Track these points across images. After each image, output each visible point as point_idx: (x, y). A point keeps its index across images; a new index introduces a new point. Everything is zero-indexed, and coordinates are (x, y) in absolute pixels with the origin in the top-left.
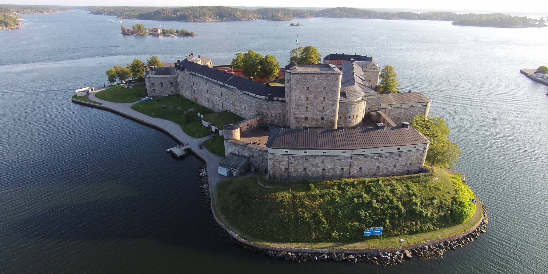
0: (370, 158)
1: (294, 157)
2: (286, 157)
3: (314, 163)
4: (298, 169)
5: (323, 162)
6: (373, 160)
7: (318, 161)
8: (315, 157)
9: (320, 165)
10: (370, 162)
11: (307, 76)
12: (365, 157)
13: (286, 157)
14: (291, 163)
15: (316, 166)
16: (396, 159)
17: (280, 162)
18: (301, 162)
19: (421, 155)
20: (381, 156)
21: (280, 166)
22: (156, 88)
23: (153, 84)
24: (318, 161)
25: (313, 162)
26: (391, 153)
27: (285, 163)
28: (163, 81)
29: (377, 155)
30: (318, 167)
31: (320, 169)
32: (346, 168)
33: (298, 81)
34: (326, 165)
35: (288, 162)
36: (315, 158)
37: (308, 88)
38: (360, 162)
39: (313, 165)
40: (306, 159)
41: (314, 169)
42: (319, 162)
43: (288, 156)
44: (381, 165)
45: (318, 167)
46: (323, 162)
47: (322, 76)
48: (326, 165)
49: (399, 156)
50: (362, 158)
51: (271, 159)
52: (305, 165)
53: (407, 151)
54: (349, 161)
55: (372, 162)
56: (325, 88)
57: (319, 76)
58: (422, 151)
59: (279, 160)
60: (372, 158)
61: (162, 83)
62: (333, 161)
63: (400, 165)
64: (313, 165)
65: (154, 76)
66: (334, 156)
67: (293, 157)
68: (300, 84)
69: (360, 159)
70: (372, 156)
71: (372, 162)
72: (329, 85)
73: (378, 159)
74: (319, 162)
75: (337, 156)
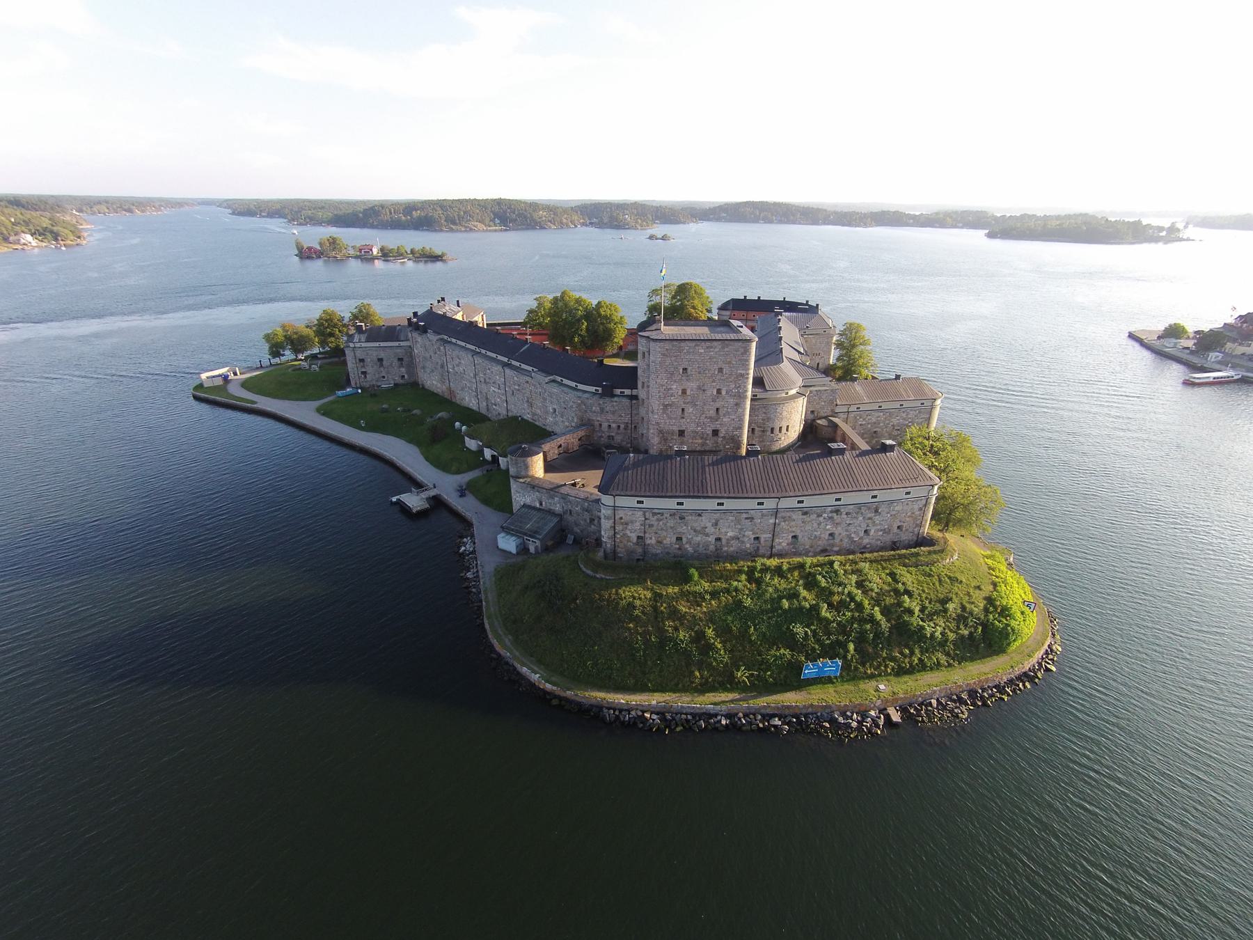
3: (697, 526)
7: (706, 521)
9: (710, 530)
11: (683, 344)
12: (805, 513)
18: (671, 523)
20: (837, 512)
22: (369, 370)
23: (362, 360)
24: (706, 521)
25: (695, 525)
26: (859, 506)
27: (637, 526)
28: (382, 355)
30: (707, 535)
31: (712, 539)
32: (765, 537)
34: (723, 530)
35: (644, 525)
37: (685, 369)
40: (682, 518)
41: (699, 539)
42: (709, 525)
43: (645, 510)
45: (707, 535)
46: (716, 524)
47: (715, 343)
48: (723, 530)
49: (876, 511)
50: (797, 516)
51: (607, 518)
52: (679, 530)
53: (892, 502)
54: (772, 521)
55: (819, 524)
56: (721, 370)
57: (708, 344)
59: (625, 519)
60: (819, 516)
61: (380, 360)
62: (738, 521)
65: (364, 345)
66: (739, 512)
67: (654, 514)
68: (668, 361)
70: (819, 511)
74: (709, 525)
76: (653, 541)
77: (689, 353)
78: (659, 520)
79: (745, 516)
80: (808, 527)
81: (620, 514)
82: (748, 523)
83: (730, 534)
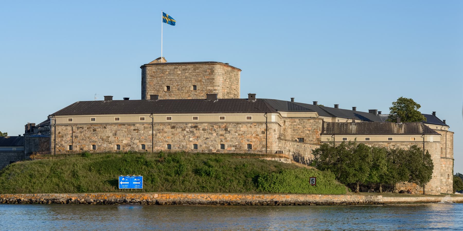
0: (179, 130)
1: (80, 127)
2: (69, 128)
4: (85, 145)
5: (116, 134)
6: (185, 132)
8: (104, 126)
9: (112, 139)
10: (181, 137)
11: (165, 68)
12: (173, 127)
13: (69, 128)
14: (76, 137)
15: (106, 140)
16: (222, 135)
17: (63, 137)
18: (88, 134)
19: (263, 133)
20: (196, 127)
21: (63, 143)
24: (108, 132)
25: (103, 135)
27: (69, 138)
29: (190, 125)
32: (148, 144)
33: (151, 76)
34: (120, 139)
35: (72, 137)
36: (105, 128)
37: (168, 88)
38: (165, 135)
40: (94, 130)
41: (105, 145)
42: (111, 135)
44: (199, 143)
45: (110, 143)
47: (189, 66)
49: (226, 130)
50: (167, 129)
53: (238, 123)
55: (184, 136)
57: (184, 67)
58: (264, 126)
60: (184, 130)
62: (129, 132)
63: (231, 146)
66: (129, 124)
69: (166, 130)
71: (184, 136)
73: (192, 132)
74: (111, 135)
75: (134, 124)
78: (81, 132)
79: (132, 128)
80: (177, 138)
82: (135, 133)
83: (125, 142)
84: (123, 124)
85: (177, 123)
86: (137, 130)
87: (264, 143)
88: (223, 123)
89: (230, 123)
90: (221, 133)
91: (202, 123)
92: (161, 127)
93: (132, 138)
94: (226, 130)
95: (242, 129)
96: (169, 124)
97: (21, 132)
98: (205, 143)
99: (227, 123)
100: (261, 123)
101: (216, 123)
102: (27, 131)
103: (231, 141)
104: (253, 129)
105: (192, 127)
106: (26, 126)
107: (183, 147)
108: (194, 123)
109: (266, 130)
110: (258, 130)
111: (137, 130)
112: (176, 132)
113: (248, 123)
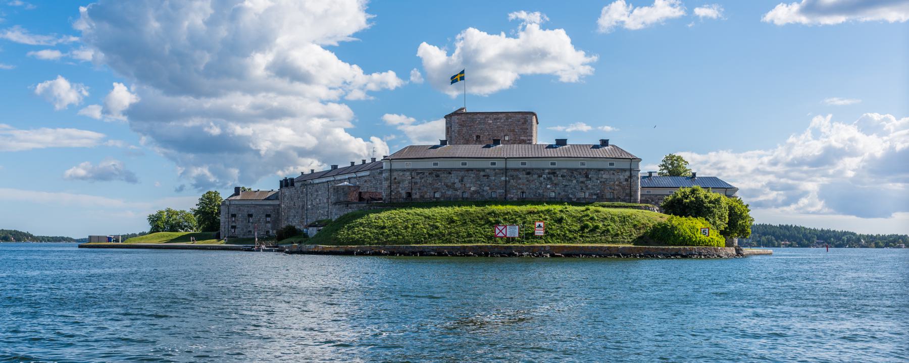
0: (536, 176)
2: (408, 173)
4: (426, 193)
6: (542, 179)
8: (449, 171)
9: (458, 185)
11: (475, 117)
12: (528, 173)
13: (408, 173)
14: (416, 183)
15: (452, 186)
16: (582, 182)
18: (430, 180)
19: (626, 180)
20: (554, 173)
23: (234, 216)
24: (454, 179)
26: (572, 171)
28: (252, 211)
30: (456, 190)
34: (468, 185)
39: (447, 186)
40: (437, 176)
42: (457, 181)
45: (456, 190)
46: (462, 181)
48: (468, 185)
49: (587, 176)
50: (522, 175)
51: (386, 179)
52: (436, 186)
53: (600, 170)
54: (503, 178)
55: (541, 183)
58: (628, 174)
60: (540, 176)
61: (250, 216)
62: (478, 178)
64: (447, 186)
66: (479, 170)
67: (418, 174)
68: (465, 130)
71: (541, 183)
72: (514, 131)
73: (549, 179)
74: (457, 181)
75: (483, 170)
76: (418, 196)
77: (480, 123)
78: (421, 178)
79: (482, 173)
81: (395, 174)
83: (473, 189)
84: (472, 170)
85: (533, 169)
86: (488, 176)
87: (628, 191)
88: (583, 169)
89: (591, 169)
90: (581, 179)
91: (560, 169)
92: (515, 173)
93: (481, 185)
94: (587, 176)
95: (604, 176)
96: (524, 170)
97: (276, 188)
98: (564, 191)
99: (588, 169)
100: (624, 170)
101: (576, 170)
102: (281, 186)
103: (593, 189)
104: (616, 177)
105: (549, 173)
106: (281, 182)
107: (539, 194)
108: (552, 169)
109: (631, 177)
110: (621, 177)
111: (488, 176)
112: (531, 179)
113: (611, 169)
